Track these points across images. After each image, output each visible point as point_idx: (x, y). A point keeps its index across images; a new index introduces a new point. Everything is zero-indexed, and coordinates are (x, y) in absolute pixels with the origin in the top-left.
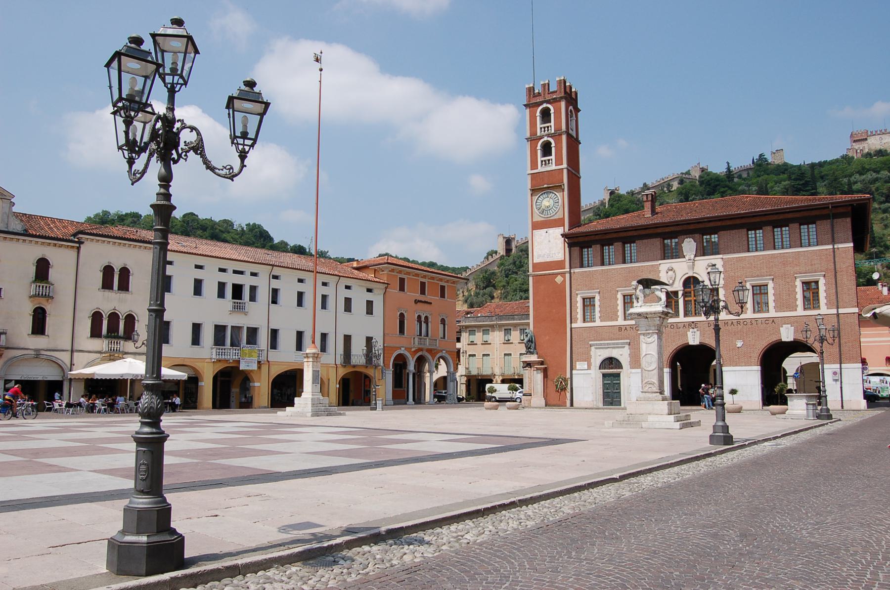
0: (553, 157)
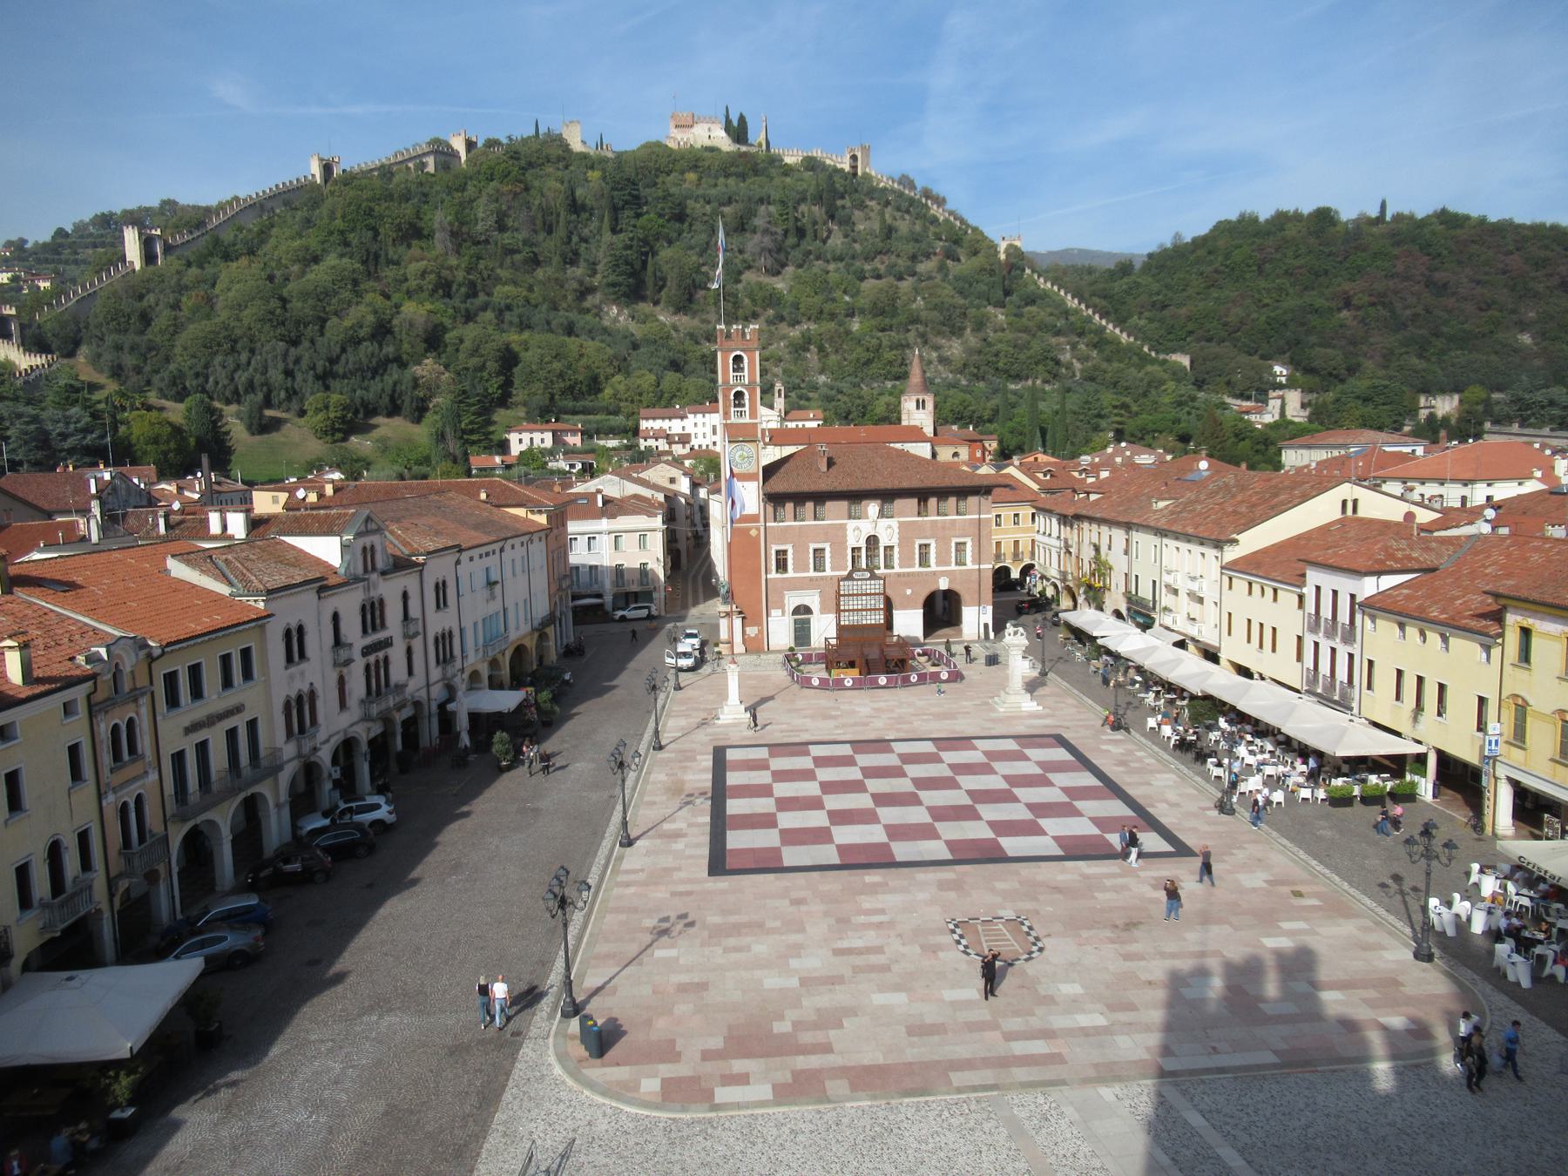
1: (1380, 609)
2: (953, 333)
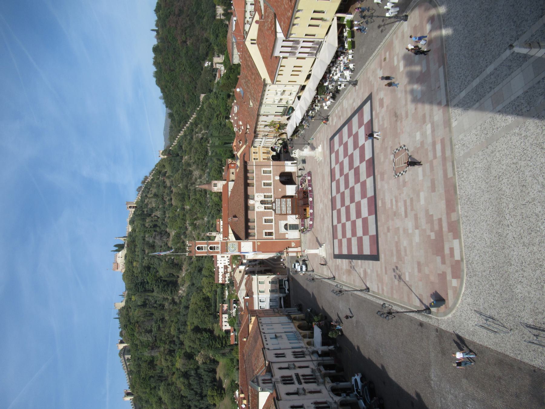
0: (216, 246)
1: (288, 32)
2: (191, 174)
